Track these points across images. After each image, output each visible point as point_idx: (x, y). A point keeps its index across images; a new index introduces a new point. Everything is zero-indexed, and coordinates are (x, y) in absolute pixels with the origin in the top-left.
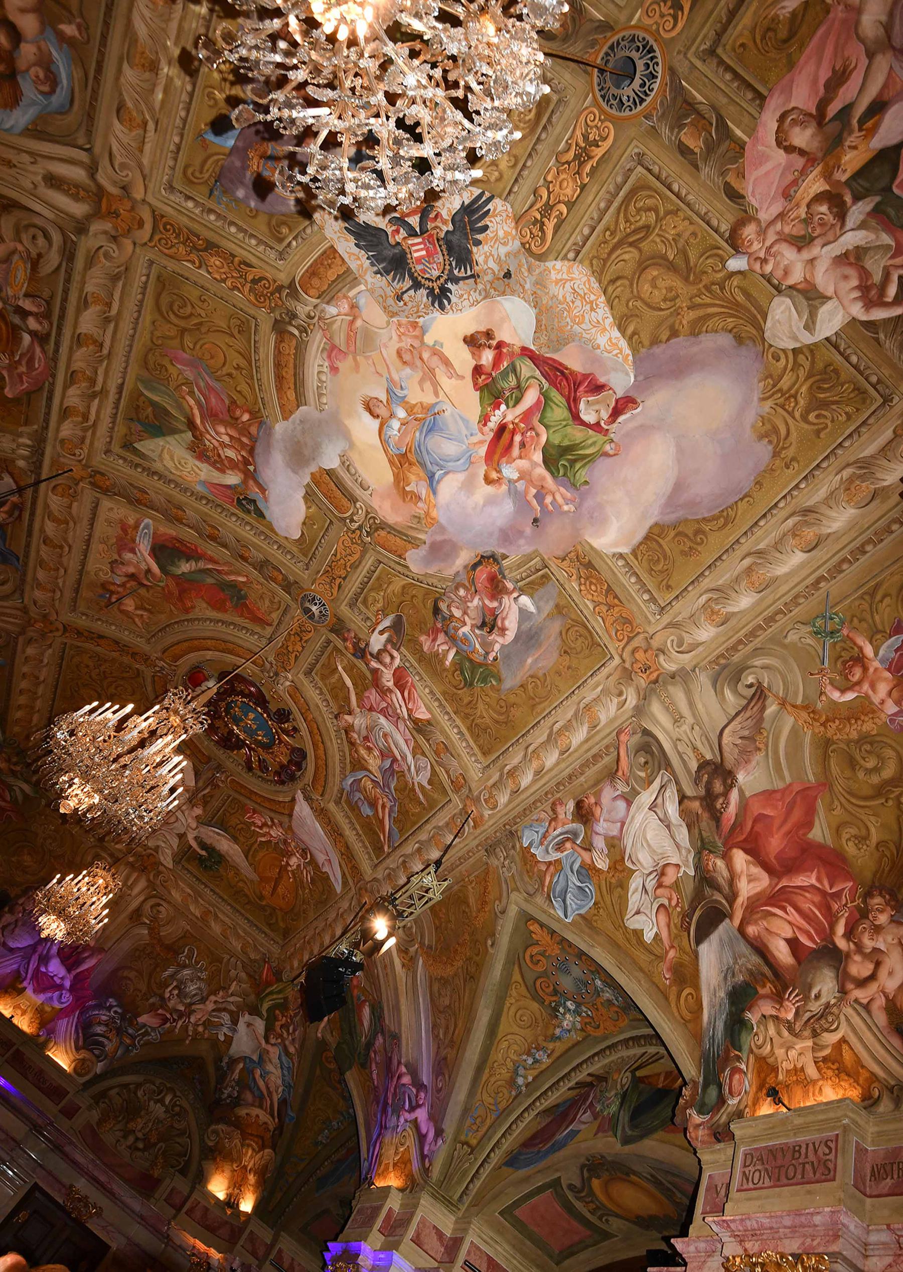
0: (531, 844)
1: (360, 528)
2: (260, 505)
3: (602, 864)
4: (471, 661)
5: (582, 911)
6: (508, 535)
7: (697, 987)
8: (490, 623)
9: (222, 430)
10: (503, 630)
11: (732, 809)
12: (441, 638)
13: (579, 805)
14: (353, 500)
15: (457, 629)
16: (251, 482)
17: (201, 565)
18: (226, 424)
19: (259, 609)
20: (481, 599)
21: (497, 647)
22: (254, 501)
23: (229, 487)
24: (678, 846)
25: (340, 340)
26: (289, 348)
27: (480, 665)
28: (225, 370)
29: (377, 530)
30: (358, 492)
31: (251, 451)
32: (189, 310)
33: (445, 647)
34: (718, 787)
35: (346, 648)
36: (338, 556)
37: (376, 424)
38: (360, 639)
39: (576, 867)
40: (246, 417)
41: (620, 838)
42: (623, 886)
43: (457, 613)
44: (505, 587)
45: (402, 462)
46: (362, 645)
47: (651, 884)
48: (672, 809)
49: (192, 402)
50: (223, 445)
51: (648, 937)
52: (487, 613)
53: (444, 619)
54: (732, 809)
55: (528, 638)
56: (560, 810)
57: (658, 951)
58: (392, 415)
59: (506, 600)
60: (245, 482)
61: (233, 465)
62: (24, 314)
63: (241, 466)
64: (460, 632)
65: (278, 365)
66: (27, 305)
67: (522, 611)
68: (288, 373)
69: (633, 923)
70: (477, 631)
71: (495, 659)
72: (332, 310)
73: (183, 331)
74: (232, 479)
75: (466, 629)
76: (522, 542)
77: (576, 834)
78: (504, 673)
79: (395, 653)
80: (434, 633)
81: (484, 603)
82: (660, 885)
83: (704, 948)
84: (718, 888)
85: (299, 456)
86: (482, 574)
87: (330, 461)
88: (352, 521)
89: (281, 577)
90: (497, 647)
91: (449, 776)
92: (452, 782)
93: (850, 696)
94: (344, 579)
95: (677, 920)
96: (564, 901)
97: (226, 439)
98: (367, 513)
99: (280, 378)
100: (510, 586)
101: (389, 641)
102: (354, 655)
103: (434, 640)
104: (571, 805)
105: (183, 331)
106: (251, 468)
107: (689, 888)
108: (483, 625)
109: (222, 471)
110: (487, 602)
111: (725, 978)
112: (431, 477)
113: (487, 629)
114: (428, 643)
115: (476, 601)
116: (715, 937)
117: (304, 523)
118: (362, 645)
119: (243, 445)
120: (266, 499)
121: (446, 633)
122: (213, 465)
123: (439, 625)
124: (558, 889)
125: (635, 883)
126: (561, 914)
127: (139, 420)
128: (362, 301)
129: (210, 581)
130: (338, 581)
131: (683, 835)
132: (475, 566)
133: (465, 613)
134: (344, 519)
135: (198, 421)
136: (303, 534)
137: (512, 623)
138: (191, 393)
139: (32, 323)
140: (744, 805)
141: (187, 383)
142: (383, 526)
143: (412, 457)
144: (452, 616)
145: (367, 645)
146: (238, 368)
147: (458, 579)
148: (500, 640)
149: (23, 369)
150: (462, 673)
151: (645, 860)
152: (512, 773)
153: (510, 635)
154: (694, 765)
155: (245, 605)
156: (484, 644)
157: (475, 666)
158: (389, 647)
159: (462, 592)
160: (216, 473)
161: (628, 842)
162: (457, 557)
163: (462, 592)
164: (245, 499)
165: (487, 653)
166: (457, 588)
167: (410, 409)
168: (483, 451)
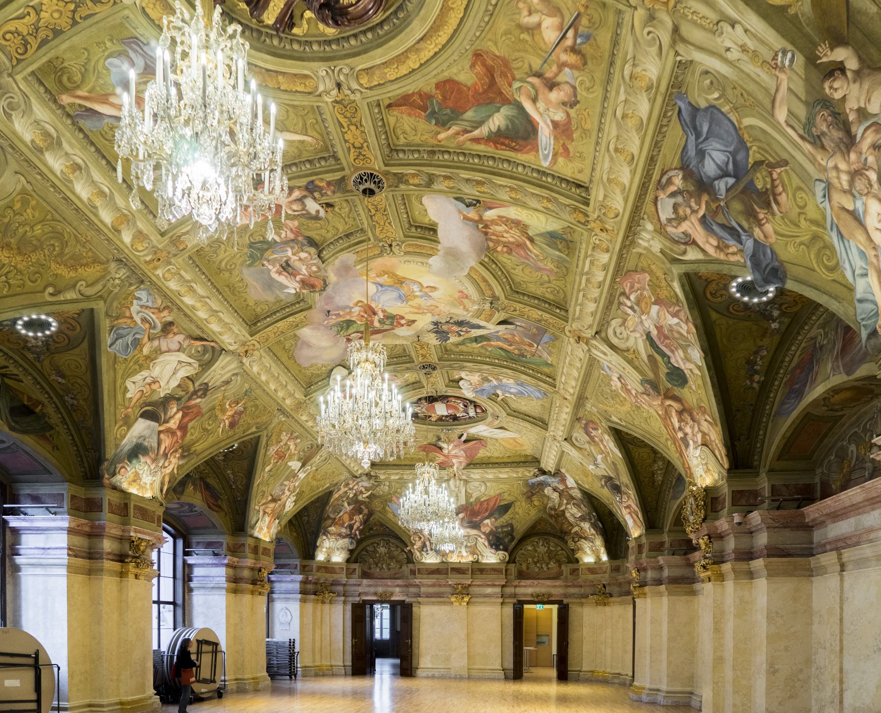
0: (139, 299)
1: (391, 246)
2: (461, 206)
3: (146, 351)
4: (267, 250)
5: (118, 354)
6: (330, 298)
7: (128, 430)
8: (287, 268)
9: (511, 240)
10: (280, 274)
11: (193, 402)
12: (291, 236)
13: (171, 324)
14: (407, 253)
15: (292, 248)
16: (477, 218)
17: (482, 131)
18: (509, 242)
19: (409, 115)
20: (304, 275)
21: (270, 267)
22: (467, 206)
23: (490, 208)
24: (168, 382)
25: (466, 301)
26: (488, 293)
27: (262, 255)
28: (521, 267)
29: (382, 251)
30: (407, 258)
31: (486, 234)
32: (549, 290)
33: (283, 235)
34: (199, 393)
35: (322, 179)
36: (387, 224)
37: (425, 285)
38: (322, 195)
39: (137, 336)
40: (499, 249)
41: (162, 353)
42: (141, 368)
43: (303, 255)
44: (305, 289)
45: (400, 281)
46: (316, 194)
47: (148, 380)
48: (183, 373)
49: (535, 251)
50: (507, 232)
51: (129, 395)
52: (294, 272)
53: (303, 245)
54: (193, 402)
55: (270, 284)
56: (166, 313)
57: (127, 404)
58: (421, 291)
59: (297, 285)
60: (481, 217)
61: (493, 222)
62: (631, 308)
63: (489, 223)
64: (289, 249)
65: (489, 285)
66: (629, 311)
67: (287, 287)
68: (482, 285)
69: (129, 384)
70: (285, 259)
71: (263, 265)
72: (476, 307)
73: (549, 282)
74: (490, 215)
75: (290, 253)
76: (323, 304)
77: (154, 328)
78: (252, 269)
79: (296, 213)
80: (297, 232)
81: (300, 274)
82: (150, 385)
83: (141, 420)
84: (165, 414)
85: (453, 255)
86: (319, 284)
87: (435, 261)
88: (398, 245)
89: (411, 181)
90: (270, 267)
91: (184, 234)
92: (180, 236)
93: (228, 407)
94: (371, 217)
95: (141, 401)
96: (116, 339)
97: (505, 235)
98: (394, 253)
99: (485, 281)
100: (305, 291)
101: (309, 213)
102: (312, 182)
103: (291, 230)
104: (169, 319)
105: (549, 282)
106: (480, 226)
107: (155, 398)
108: (288, 265)
109: (500, 217)
110: (301, 277)
111: (140, 437)
112: (381, 286)
113: (284, 265)
114: (291, 225)
115: (304, 271)
116: (148, 423)
117: (426, 210)
118: (316, 194)
119: (493, 234)
120: (460, 212)
121: (292, 240)
122: (508, 220)
123: (300, 239)
124: (120, 331)
125: (145, 373)
126: (109, 342)
127: (566, 241)
128: (465, 313)
129: (469, 114)
130: (373, 212)
131: (174, 383)
132: (325, 281)
133: (300, 259)
134: (403, 242)
135: (528, 243)
136: (421, 204)
137: (282, 279)
138: (537, 256)
139: (629, 303)
140: (196, 405)
141: (541, 261)
142: (381, 255)
143: (398, 285)
144: (302, 251)
145: (315, 199)
146: (514, 269)
147: (323, 271)
148: (275, 270)
149: (637, 286)
150: (260, 242)
151: (156, 371)
152: (192, 290)
153: (275, 276)
154: (206, 381)
155: (424, 109)
156: (275, 260)
157: (263, 251)
158: (304, 212)
159: (314, 268)
160: (503, 214)
161: (161, 358)
162: (335, 275)
163: (314, 268)
164: (475, 205)
165: (268, 261)
166: (318, 268)
167: (416, 297)
168: (373, 305)
